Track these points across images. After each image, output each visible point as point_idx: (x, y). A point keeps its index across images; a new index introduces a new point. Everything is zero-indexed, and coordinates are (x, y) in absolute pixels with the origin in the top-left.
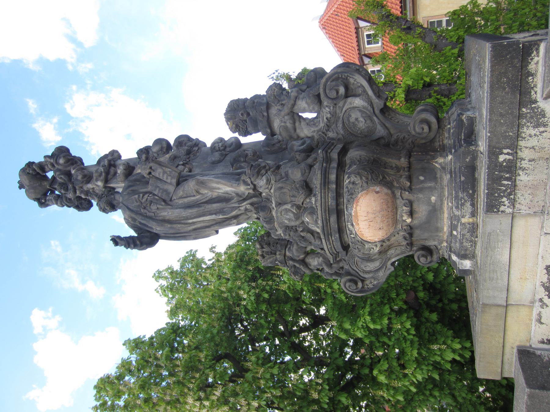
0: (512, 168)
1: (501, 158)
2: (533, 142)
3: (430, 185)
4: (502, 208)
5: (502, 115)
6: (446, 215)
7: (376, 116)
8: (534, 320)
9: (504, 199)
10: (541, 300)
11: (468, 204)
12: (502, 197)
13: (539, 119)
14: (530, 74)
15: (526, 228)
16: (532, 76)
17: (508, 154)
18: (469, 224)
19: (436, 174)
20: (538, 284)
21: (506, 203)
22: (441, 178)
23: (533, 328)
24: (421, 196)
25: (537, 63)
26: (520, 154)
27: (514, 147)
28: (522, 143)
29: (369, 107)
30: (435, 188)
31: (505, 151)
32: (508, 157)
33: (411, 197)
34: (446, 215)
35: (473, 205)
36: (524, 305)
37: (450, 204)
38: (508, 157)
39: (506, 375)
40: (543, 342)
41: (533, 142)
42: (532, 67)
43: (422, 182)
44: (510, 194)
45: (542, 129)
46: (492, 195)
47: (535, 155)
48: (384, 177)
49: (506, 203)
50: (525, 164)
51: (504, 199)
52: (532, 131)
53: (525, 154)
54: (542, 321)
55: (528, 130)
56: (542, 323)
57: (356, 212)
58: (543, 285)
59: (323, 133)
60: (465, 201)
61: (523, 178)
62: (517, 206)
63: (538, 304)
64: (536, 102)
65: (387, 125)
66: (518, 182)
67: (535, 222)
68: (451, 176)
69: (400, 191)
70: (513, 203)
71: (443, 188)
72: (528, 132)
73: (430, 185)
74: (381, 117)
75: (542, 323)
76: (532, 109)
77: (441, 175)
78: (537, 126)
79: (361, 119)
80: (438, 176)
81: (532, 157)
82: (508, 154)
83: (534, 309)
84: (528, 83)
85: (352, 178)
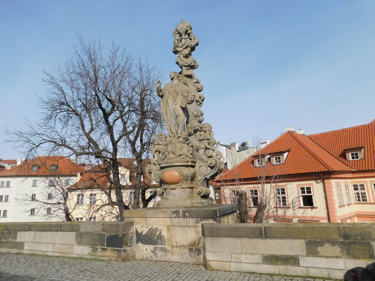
1: (187, 214)
2: (191, 221)
4: (173, 215)
5: (198, 213)
9: (176, 215)
12: (176, 214)
13: (197, 222)
14: (208, 219)
15: (168, 221)
16: (208, 220)
17: (188, 215)
21: (175, 216)
25: (211, 221)
27: (189, 217)
31: (189, 214)
32: (187, 215)
38: (187, 215)
39: (125, 218)
40: (136, 228)
41: (191, 221)
42: (210, 220)
45: (194, 223)
46: (177, 212)
49: (175, 216)
51: (176, 215)
52: (194, 221)
55: (194, 220)
58: (152, 227)
61: (182, 219)
63: (147, 226)
64: (201, 221)
76: (200, 221)
81: (187, 221)
82: (188, 215)
84: (206, 219)
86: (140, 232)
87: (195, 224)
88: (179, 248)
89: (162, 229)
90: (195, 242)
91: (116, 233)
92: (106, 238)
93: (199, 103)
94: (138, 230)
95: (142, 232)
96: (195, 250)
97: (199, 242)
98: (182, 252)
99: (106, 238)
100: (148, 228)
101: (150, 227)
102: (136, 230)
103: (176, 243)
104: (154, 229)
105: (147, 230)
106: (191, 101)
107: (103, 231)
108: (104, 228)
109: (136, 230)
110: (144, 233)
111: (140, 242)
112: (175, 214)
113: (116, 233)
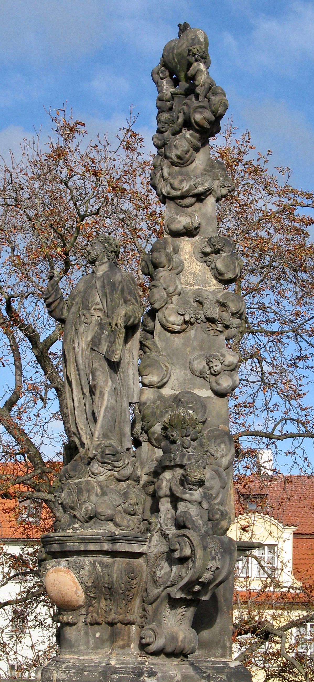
3: (91, 642)
7: (165, 589)
18: (53, 677)
19: (101, 649)
22: (97, 654)
24: (82, 633)
29: (170, 583)
30: (88, 648)
33: (81, 624)
37: (72, 661)
43: (94, 635)
48: (94, 598)
59: (160, 529)
60: (67, 674)
65: (158, 600)
68: (96, 663)
69: (85, 613)
71: (87, 655)
73: (91, 642)
74: (164, 594)
77: (99, 653)
79: (163, 572)
80: (99, 651)
85: (89, 566)
93: (220, 327)
106: (185, 322)
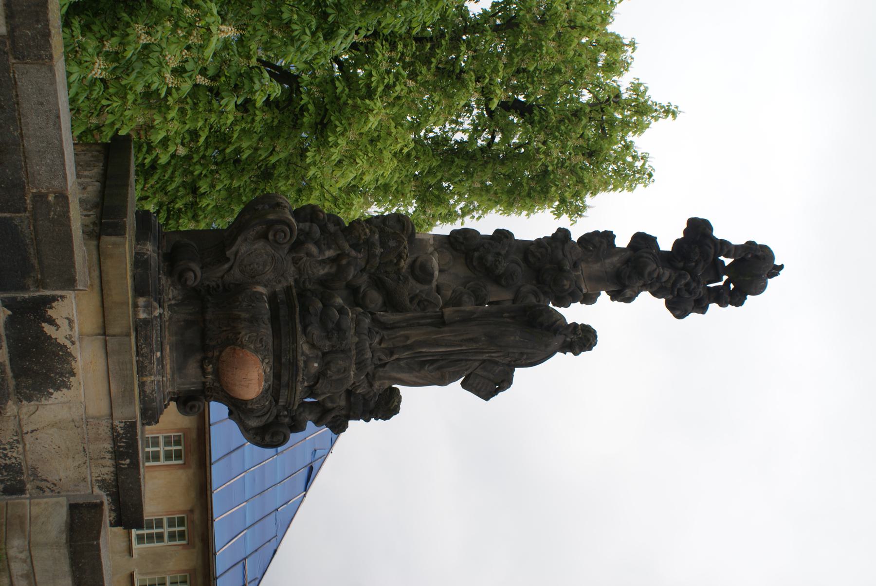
0: (117, 455)
1: (128, 461)
2: (105, 470)
4: (122, 425)
6: (168, 367)
8: (76, 320)
9: (121, 432)
10: (73, 343)
11: (148, 391)
13: (103, 484)
14: (114, 511)
20: (79, 358)
23: (74, 312)
26: (113, 462)
28: (112, 469)
34: (168, 367)
35: (144, 391)
36: (88, 336)
40: (62, 297)
42: (113, 515)
44: (117, 436)
47: (100, 461)
50: (108, 456)
53: (109, 462)
54: (67, 321)
55: (109, 477)
56: (67, 318)
57: (260, 385)
58: (74, 358)
61: (108, 446)
62: (110, 425)
64: (107, 495)
66: (111, 442)
67: (92, 411)
70: (113, 428)
72: (109, 476)
75: (67, 318)
78: (103, 481)
83: (77, 332)
86: (50, 312)
87: (97, 481)
88: (15, 438)
89: (69, 388)
90: (45, 480)
91: (37, 266)
92: (7, 215)
94: (54, 304)
95: (52, 322)
96: (20, 480)
97: (46, 489)
98: (8, 447)
99: (7, 215)
100: (68, 344)
101: (72, 349)
102: (54, 299)
103: (32, 431)
104: (69, 363)
105: (62, 340)
107: (35, 196)
108: (48, 203)
109: (54, 299)
110: (47, 328)
111: (10, 313)
112: (124, 428)
113: (37, 266)
